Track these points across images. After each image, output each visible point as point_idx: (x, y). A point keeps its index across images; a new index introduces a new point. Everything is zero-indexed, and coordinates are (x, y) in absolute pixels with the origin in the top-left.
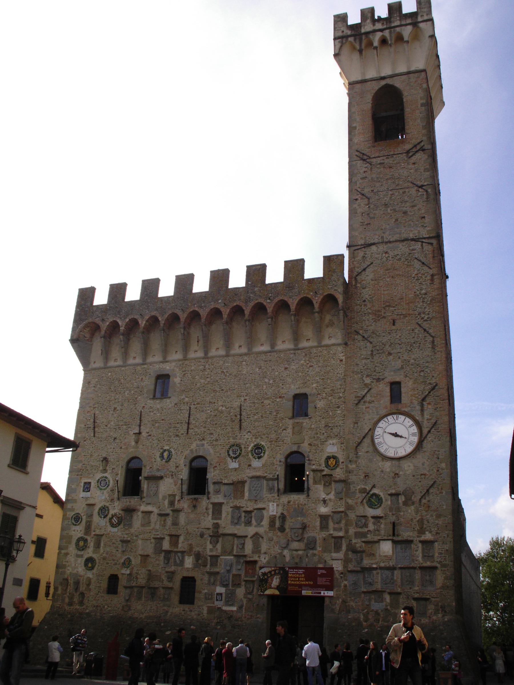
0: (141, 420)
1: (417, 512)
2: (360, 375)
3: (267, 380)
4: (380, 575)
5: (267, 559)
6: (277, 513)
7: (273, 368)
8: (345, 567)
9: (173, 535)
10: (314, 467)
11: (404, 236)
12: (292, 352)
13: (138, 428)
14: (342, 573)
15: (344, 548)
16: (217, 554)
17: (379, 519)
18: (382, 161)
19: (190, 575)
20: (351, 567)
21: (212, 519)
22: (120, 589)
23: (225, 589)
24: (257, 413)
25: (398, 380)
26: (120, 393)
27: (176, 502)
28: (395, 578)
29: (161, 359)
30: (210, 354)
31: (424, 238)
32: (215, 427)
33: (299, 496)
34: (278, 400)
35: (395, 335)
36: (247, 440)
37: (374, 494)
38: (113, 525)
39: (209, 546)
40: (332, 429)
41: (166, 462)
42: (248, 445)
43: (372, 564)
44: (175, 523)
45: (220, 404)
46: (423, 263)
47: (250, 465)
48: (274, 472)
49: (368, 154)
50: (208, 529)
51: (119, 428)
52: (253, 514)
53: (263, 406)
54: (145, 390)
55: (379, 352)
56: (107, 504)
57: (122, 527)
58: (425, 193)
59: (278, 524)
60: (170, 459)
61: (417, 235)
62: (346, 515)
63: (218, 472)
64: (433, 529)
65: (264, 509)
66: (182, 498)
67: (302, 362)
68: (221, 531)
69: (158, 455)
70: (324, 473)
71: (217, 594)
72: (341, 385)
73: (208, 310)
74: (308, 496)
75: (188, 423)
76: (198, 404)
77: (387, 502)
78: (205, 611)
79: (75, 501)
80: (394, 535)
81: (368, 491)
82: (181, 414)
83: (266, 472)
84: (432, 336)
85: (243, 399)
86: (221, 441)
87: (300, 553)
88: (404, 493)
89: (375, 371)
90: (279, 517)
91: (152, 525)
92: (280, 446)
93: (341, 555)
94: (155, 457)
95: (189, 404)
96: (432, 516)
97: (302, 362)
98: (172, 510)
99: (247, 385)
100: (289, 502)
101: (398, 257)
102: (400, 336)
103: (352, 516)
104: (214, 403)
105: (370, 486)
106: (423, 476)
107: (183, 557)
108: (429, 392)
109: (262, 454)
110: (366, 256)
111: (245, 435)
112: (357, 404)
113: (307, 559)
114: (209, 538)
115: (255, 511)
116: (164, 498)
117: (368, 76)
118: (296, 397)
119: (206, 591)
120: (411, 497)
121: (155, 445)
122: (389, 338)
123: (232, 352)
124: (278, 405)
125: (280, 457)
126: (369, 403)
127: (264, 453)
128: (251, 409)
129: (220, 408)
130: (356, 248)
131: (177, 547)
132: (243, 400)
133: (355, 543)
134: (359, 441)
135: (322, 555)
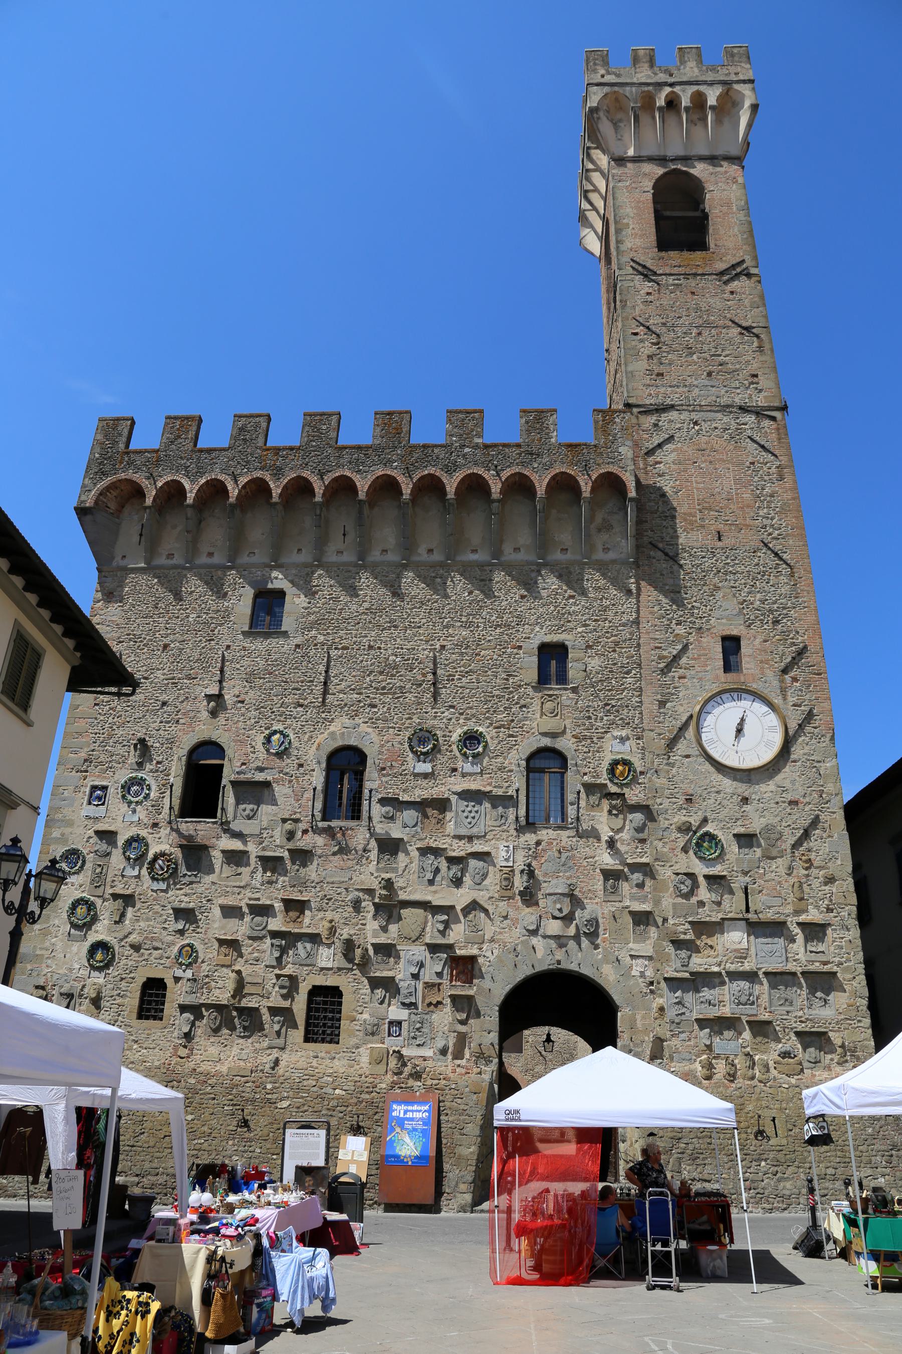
1: (790, 870)
12: (533, 567)
19: (329, 983)
21: (378, 870)
22: (170, 1009)
24: (467, 672)
25: (735, 632)
32: (382, 694)
34: (508, 651)
46: (763, 447)
49: (651, 268)
50: (370, 892)
56: (143, 833)
61: (747, 400)
65: (488, 854)
69: (260, 739)
71: (391, 1023)
73: (370, 478)
76: (344, 648)
78: (365, 1059)
79: (70, 823)
80: (748, 910)
83: (490, 784)
90: (522, 871)
92: (516, 736)
94: (254, 744)
100: (538, 843)
104: (379, 648)
109: (480, 749)
111: (443, 713)
112: (662, 670)
113: (580, 954)
119: (366, 1016)
121: (253, 721)
122: (713, 561)
123: (415, 558)
125: (516, 758)
132: (438, 647)
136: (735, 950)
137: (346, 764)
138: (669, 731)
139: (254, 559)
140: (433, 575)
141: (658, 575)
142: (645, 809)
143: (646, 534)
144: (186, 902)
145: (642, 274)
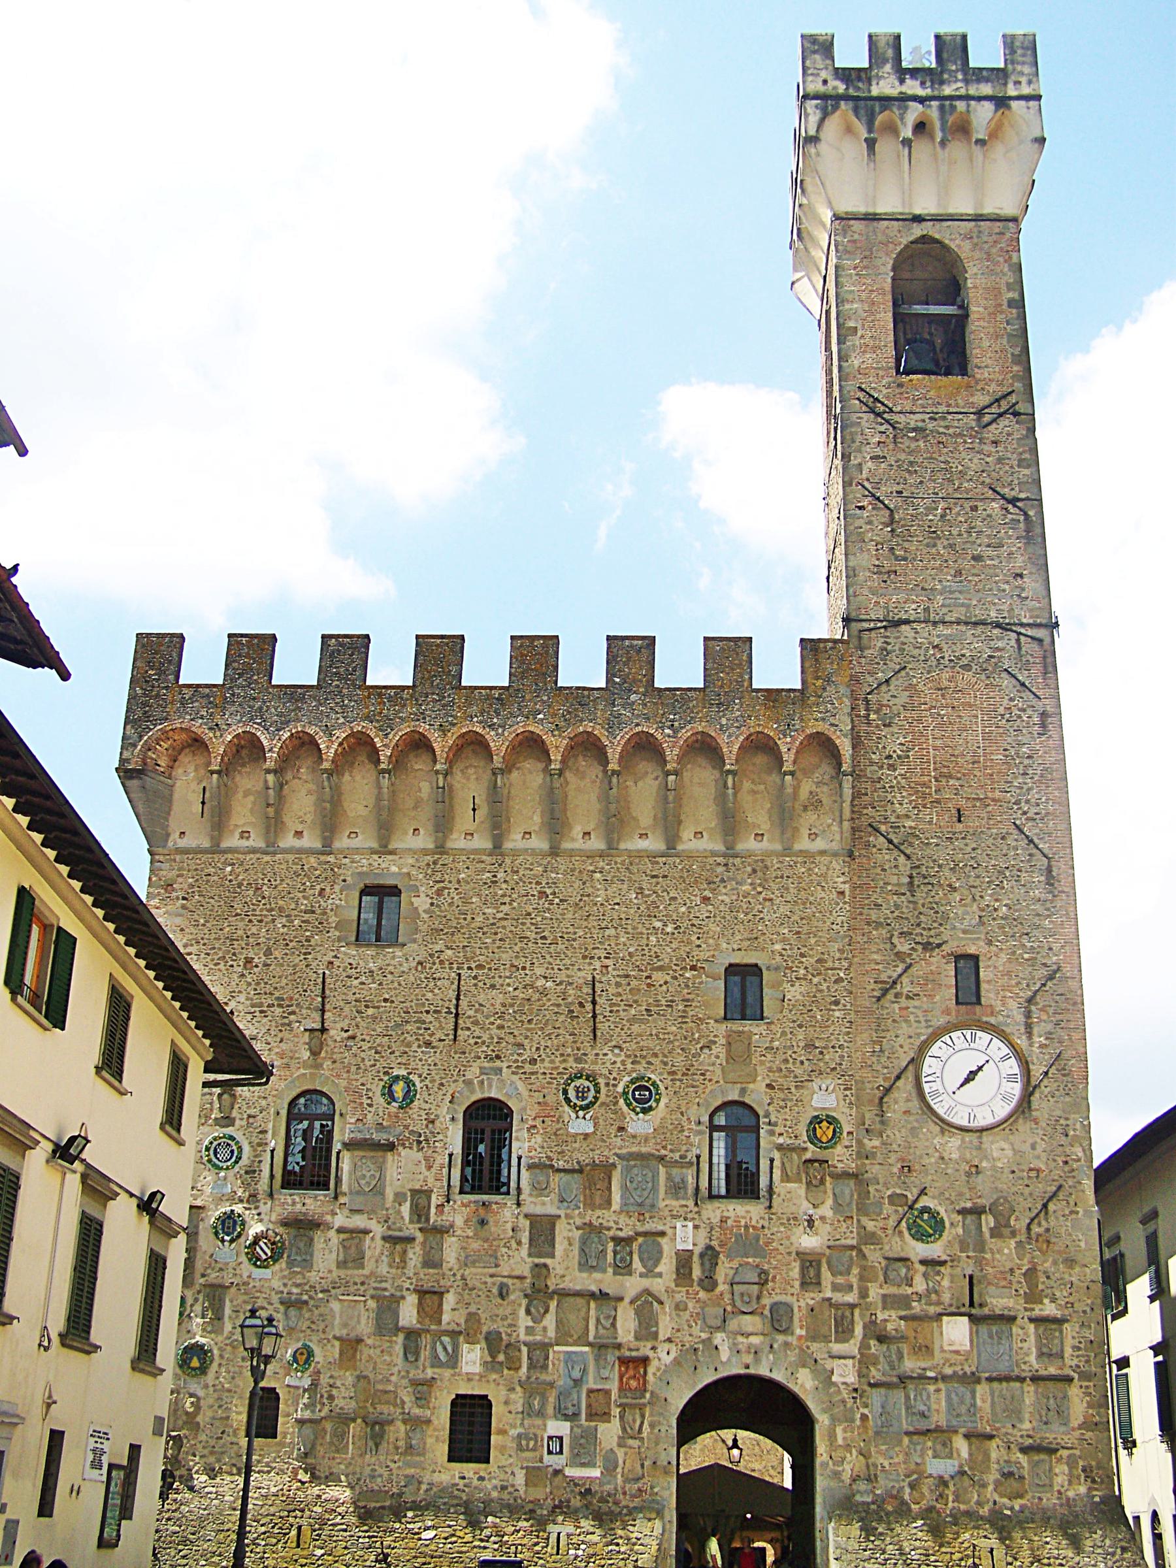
0: (323, 998)
2: (884, 932)
3: (658, 924)
4: (943, 1393)
5: (673, 1355)
6: (694, 1245)
7: (671, 895)
9: (426, 1292)
10: (781, 1140)
11: (978, 614)
12: (719, 860)
13: (317, 1016)
14: (856, 1390)
15: (859, 1330)
16: (546, 1340)
17: (938, 1268)
18: (920, 424)
20: (875, 1374)
21: (530, 1255)
23: (568, 1424)
25: (972, 950)
26: (260, 921)
27: (433, 1210)
28: (979, 1402)
29: (375, 845)
30: (508, 845)
31: (1022, 625)
33: (748, 1208)
35: (962, 846)
36: (612, 1064)
37: (925, 1210)
38: (255, 1260)
39: (524, 1321)
40: (821, 1053)
41: (401, 1107)
42: (615, 1079)
43: (924, 1369)
44: (432, 1262)
45: (539, 971)
47: (621, 1129)
48: (684, 1148)
50: (521, 1278)
51: (261, 1012)
52: (635, 1246)
53: (649, 985)
54: (333, 919)
56: (238, 1208)
57: (284, 1265)
58: (1022, 518)
59: (697, 1273)
60: (412, 1101)
61: (1006, 614)
64: (1058, 1294)
65: (662, 1234)
66: (448, 1202)
67: (746, 888)
68: (552, 1284)
69: (377, 1089)
70: (808, 1155)
72: (841, 951)
74: (770, 1207)
75: (457, 1015)
76: (480, 967)
77: (954, 1228)
78: (520, 1479)
80: (972, 1304)
81: (910, 1203)
82: (436, 991)
83: (664, 1148)
85: (597, 964)
86: (547, 1064)
87: (755, 1340)
89: (919, 925)
90: (702, 1255)
93: (852, 1347)
94: (371, 1094)
95: (455, 966)
96: (1055, 1263)
97: (746, 888)
98: (420, 1229)
99: (607, 932)
101: (965, 661)
102: (974, 849)
103: (874, 1256)
105: (916, 1191)
106: (1033, 1174)
107: (456, 1348)
108: (1044, 985)
109: (652, 1103)
110: (889, 648)
111: (605, 1055)
113: (771, 1356)
114: (524, 1302)
115: (640, 1240)
116: (399, 1198)
117: (883, 207)
118: (732, 970)
121: (368, 1063)
123: (566, 845)
124: (687, 986)
126: (908, 997)
127: (658, 1101)
128: (620, 990)
129: (540, 983)
130: (866, 625)
131: (440, 1322)
133: (886, 1320)
134: (887, 1085)
135: (808, 1348)
137: (488, 1122)
138: (885, 1079)
139: (356, 843)
140: (591, 868)
141: (878, 870)
143: (865, 811)
145: (872, 411)
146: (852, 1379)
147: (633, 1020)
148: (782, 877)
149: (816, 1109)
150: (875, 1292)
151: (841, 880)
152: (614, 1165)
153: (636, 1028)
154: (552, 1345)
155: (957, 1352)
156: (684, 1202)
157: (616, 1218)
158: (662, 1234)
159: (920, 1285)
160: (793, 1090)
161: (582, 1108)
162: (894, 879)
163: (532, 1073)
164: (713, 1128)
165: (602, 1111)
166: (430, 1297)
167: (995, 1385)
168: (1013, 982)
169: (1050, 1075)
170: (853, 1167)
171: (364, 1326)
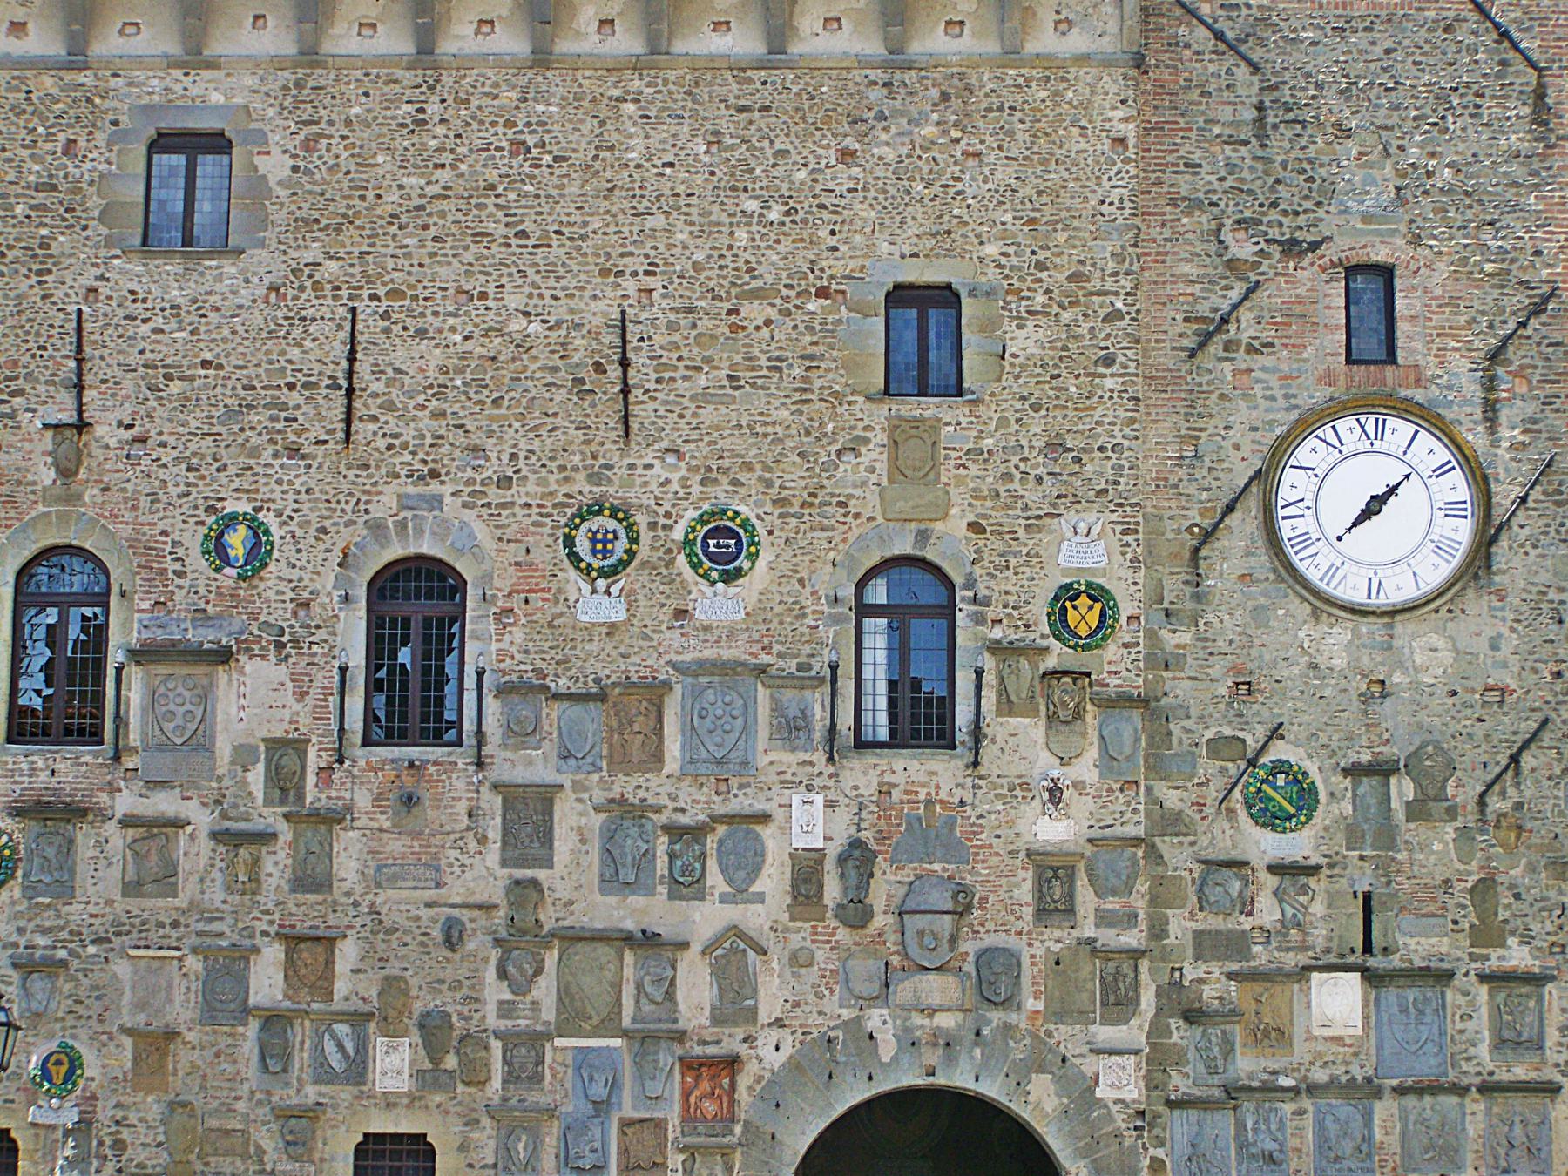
0: (80, 361)
2: (1204, 219)
3: (752, 205)
4: (1309, 1119)
7: (778, 146)
8: (1152, 1085)
9: (301, 939)
10: (997, 633)
12: (875, 74)
13: (67, 398)
14: (1141, 1113)
15: (1148, 1000)
16: (539, 1028)
17: (1303, 880)
20: (1179, 1083)
21: (504, 863)
25: (1380, 255)
27: (311, 779)
28: (1378, 1135)
29: (174, 48)
30: (447, 47)
33: (933, 765)
35: (1364, 45)
36: (663, 487)
37: (1280, 767)
39: (495, 992)
40: (1077, 460)
42: (668, 515)
43: (1274, 1073)
44: (311, 878)
45: (514, 301)
47: (681, 613)
48: (807, 649)
50: (487, 907)
52: (711, 842)
53: (735, 328)
54: (95, 203)
55: (1291, 116)
57: (17, 893)
59: (832, 891)
62: (1155, 856)
63: (518, 635)
64: (1536, 927)
65: (765, 818)
66: (340, 761)
67: (929, 131)
68: (549, 918)
69: (193, 542)
70: (1051, 663)
72: (1119, 257)
74: (976, 764)
75: (350, 391)
76: (395, 294)
77: (1337, 802)
80: (1368, 948)
81: (1249, 755)
82: (308, 344)
84: (1533, 65)
85: (630, 287)
86: (531, 487)
87: (946, 1021)
88: (1411, 765)
89: (1274, 205)
90: (842, 860)
91: (188, 890)
93: (1134, 1032)
94: (180, 552)
95: (344, 293)
96: (1532, 868)
97: (929, 131)
98: (287, 817)
99: (650, 222)
102: (1388, 52)
103: (1178, 857)
105: (1261, 732)
106: (1493, 697)
107: (362, 1046)
108: (1523, 325)
111: (648, 467)
113: (978, 1051)
114: (494, 955)
115: (722, 830)
116: (243, 757)
120: (1444, 787)
123: (564, 46)
124: (811, 329)
126: (1251, 350)
127: (753, 557)
128: (676, 337)
129: (517, 325)
131: (328, 996)
132: (632, 292)
133: (1201, 981)
134: (1207, 523)
135: (1049, 1034)
136: (1332, 1039)
137: (416, 603)
140: (616, 93)
142: (1143, 702)
144: (45, 948)
146: (1133, 1092)
147: (704, 398)
148: (1001, 109)
149: (1066, 572)
150: (1180, 927)
151: (1120, 114)
152: (667, 686)
153: (708, 414)
154: (549, 1037)
155: (1338, 1040)
156: (806, 757)
157: (674, 789)
158: (765, 818)
159: (1267, 912)
160: (1021, 533)
161: (603, 573)
162: (1226, 113)
163: (503, 506)
164: (863, 610)
165: (644, 577)
166: (308, 948)
167: (1411, 1101)
168: (1462, 319)
169: (1531, 504)
170: (1137, 683)
171: (181, 1009)
